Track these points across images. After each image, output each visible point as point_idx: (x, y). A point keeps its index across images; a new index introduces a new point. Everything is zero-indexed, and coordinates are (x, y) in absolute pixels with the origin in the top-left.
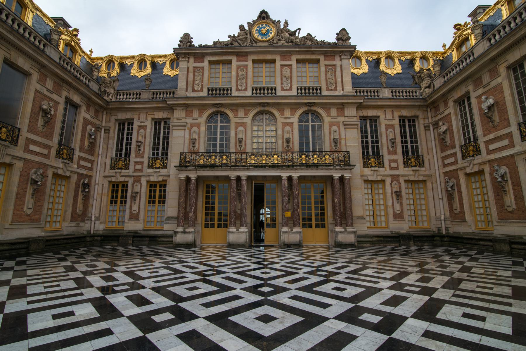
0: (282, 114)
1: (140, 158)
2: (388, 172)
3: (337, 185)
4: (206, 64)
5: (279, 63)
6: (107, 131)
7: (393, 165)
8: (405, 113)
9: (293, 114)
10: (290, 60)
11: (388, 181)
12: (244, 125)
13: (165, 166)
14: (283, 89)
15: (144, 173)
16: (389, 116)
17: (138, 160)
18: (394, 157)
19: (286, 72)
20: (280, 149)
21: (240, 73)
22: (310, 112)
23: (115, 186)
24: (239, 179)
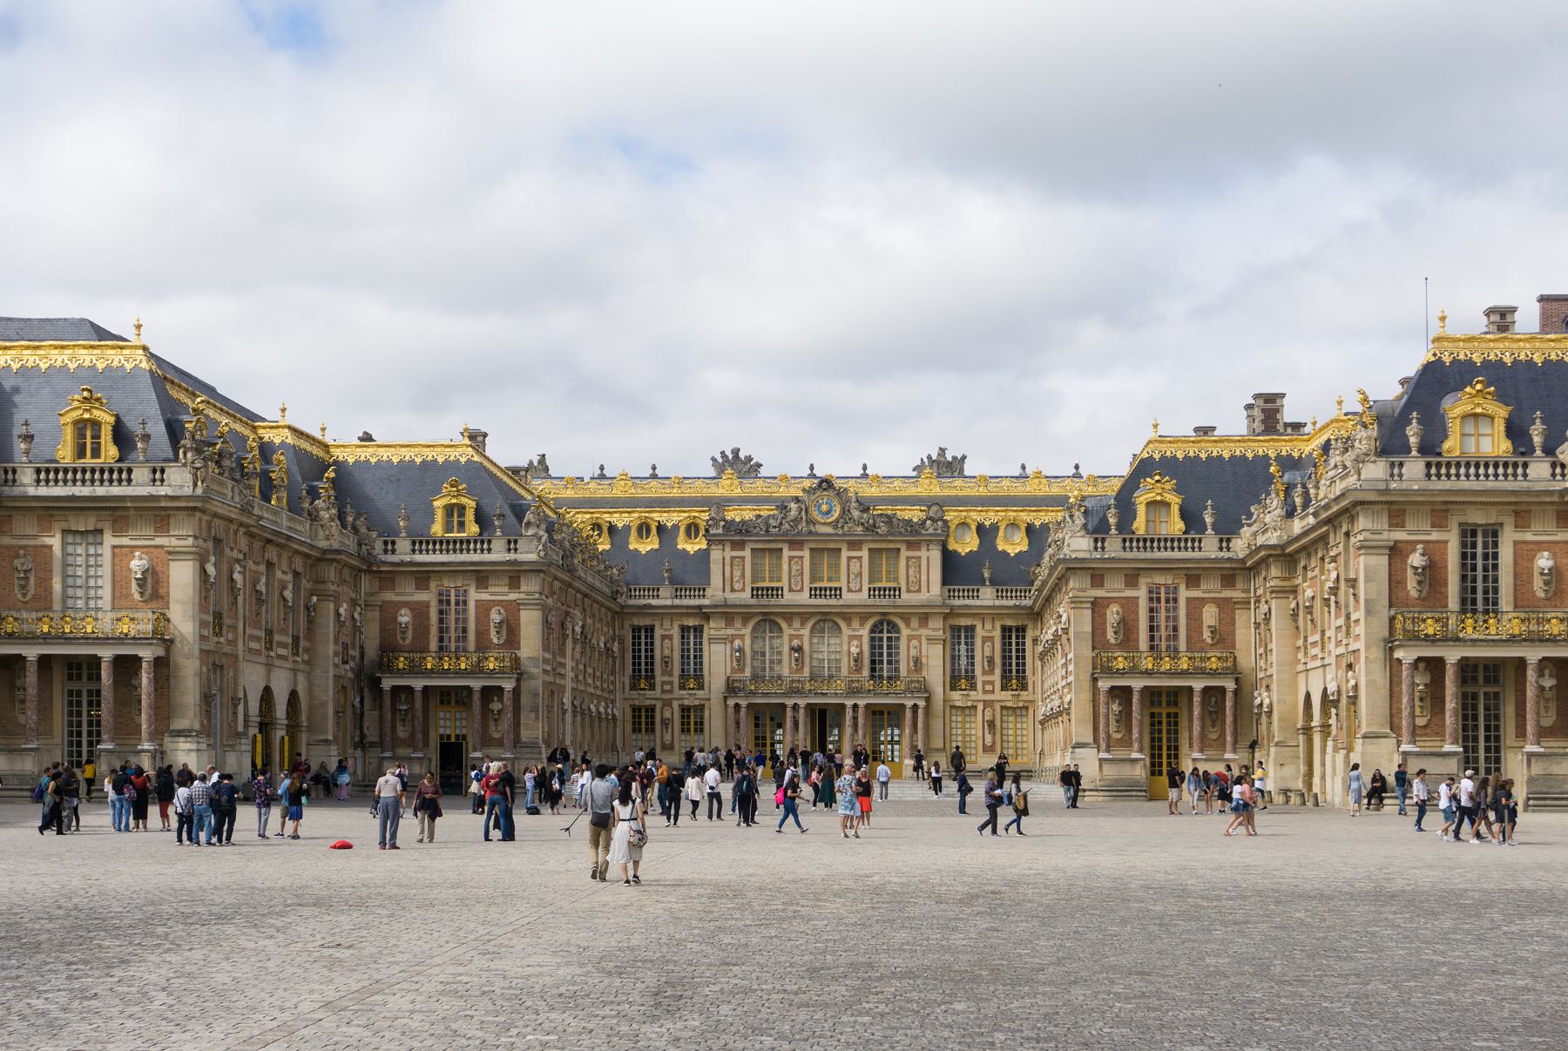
0: (849, 625)
1: (666, 678)
2: (982, 697)
3: (908, 714)
4: (747, 553)
5: (845, 554)
6: (622, 642)
7: (989, 687)
8: (1009, 623)
9: (862, 625)
10: (860, 549)
11: (980, 707)
12: (800, 637)
13: (701, 687)
14: (850, 590)
15: (675, 695)
16: (988, 626)
17: (666, 678)
18: (990, 678)
19: (855, 566)
20: (844, 672)
21: (794, 568)
22: (884, 626)
23: (636, 710)
24: (795, 707)
